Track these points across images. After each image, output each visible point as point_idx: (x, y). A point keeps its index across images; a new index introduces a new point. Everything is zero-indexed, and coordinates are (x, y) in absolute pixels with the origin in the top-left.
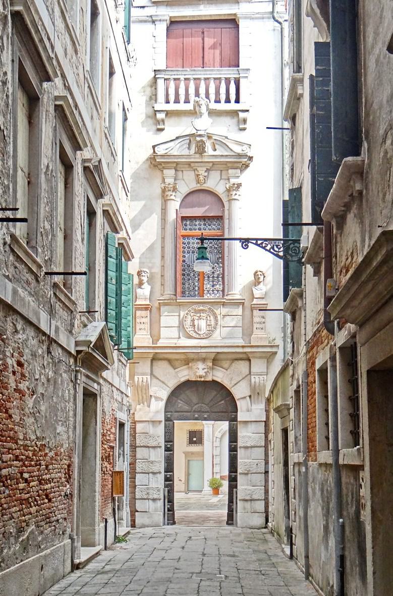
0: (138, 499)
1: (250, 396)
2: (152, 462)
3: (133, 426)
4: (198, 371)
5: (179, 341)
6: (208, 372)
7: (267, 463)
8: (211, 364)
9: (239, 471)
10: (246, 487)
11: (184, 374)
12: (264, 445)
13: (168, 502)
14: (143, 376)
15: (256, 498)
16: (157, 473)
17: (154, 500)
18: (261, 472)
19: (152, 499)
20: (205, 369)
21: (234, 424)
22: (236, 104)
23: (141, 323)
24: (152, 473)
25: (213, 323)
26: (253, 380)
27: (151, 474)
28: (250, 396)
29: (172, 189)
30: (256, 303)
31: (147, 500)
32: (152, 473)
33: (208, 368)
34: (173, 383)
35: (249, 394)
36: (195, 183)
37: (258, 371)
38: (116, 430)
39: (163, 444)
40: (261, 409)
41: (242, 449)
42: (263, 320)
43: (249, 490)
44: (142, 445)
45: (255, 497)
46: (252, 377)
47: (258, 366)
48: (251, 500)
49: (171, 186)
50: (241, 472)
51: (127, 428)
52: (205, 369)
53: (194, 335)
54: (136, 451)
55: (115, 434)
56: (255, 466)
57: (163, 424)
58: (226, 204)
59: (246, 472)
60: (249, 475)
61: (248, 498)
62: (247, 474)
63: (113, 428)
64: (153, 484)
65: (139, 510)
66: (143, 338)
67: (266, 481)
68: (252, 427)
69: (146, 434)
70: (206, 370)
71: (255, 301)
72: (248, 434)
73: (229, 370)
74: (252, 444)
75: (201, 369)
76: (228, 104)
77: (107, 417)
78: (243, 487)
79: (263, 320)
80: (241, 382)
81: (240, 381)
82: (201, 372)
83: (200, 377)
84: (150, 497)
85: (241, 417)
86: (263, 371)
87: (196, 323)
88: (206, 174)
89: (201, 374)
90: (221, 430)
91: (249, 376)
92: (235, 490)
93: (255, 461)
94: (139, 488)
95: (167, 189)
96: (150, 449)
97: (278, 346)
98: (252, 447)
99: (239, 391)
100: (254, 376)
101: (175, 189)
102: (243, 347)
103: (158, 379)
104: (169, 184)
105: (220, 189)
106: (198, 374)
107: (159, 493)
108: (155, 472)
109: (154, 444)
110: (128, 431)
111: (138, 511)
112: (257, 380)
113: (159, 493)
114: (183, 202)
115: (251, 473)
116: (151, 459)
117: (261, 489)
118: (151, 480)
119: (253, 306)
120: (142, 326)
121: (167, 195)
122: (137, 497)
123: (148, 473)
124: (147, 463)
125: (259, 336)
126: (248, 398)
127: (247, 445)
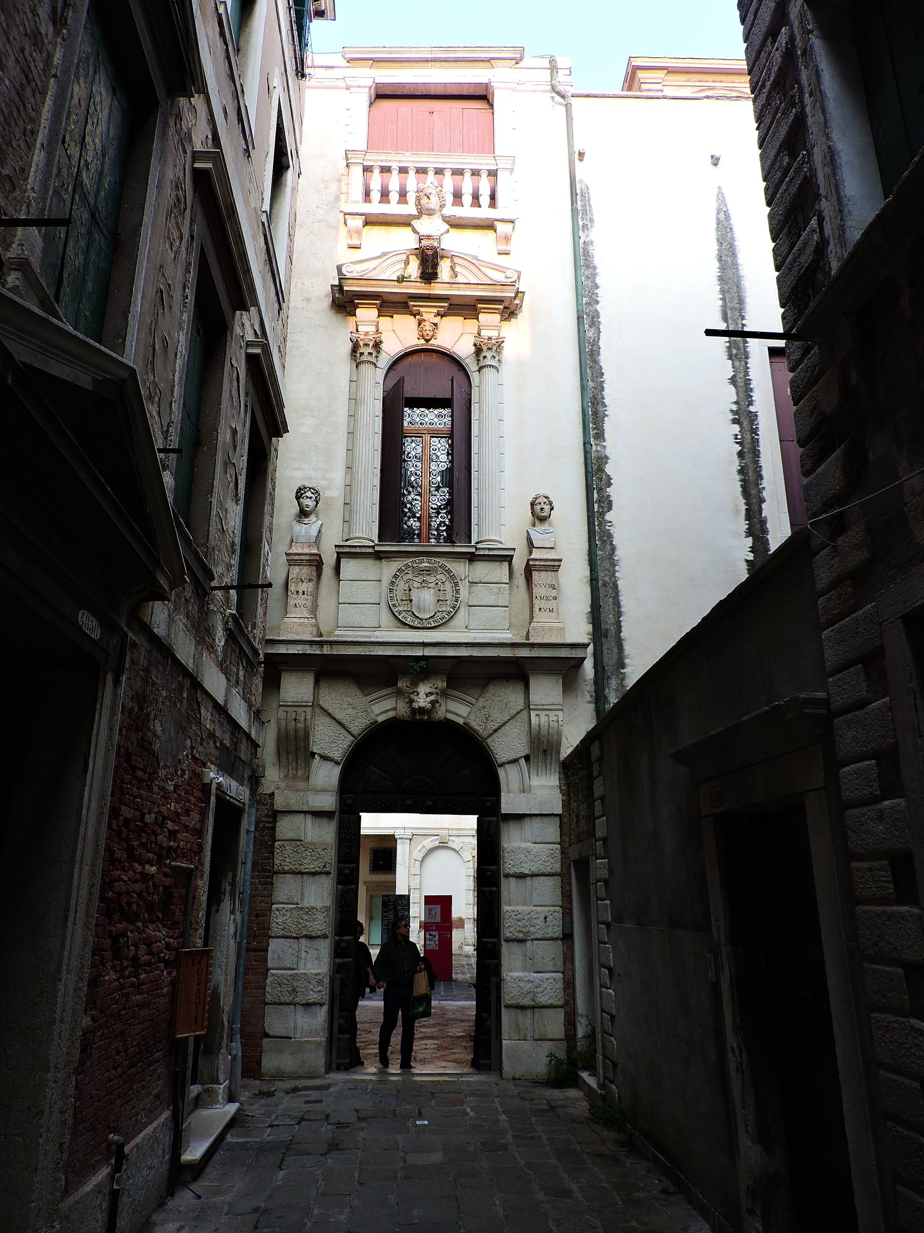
0: (270, 1004)
1: (527, 758)
2: (310, 911)
3: (268, 822)
4: (415, 698)
5: (376, 633)
6: (437, 702)
7: (567, 913)
8: (445, 684)
9: (507, 933)
10: (520, 974)
11: (383, 708)
12: (559, 870)
13: (341, 1010)
14: (299, 710)
15: (544, 1003)
16: (318, 937)
17: (307, 1005)
18: (555, 936)
19: (303, 1005)
20: (431, 694)
21: (490, 822)
22: (491, 209)
23: (298, 592)
24: (306, 936)
25: (449, 597)
26: (534, 720)
27: (303, 941)
28: (527, 758)
29: (371, 344)
30: (538, 557)
31: (293, 1007)
32: (306, 936)
33: (437, 694)
34: (358, 725)
35: (526, 752)
36: (417, 336)
37: (545, 702)
38: (203, 819)
39: (332, 868)
40: (550, 787)
41: (513, 881)
42: (554, 593)
43: (529, 981)
44: (286, 868)
45: (543, 999)
46: (533, 714)
47: (545, 691)
48: (533, 1007)
49: (371, 337)
50: (509, 935)
51: (248, 823)
52: (431, 694)
53: (409, 620)
54: (272, 884)
55: (199, 833)
56: (540, 922)
57: (337, 814)
58: (475, 378)
59: (521, 935)
60: (529, 944)
61: (526, 1001)
62: (522, 941)
63: (195, 816)
64: (309, 965)
65: (271, 1033)
66: (301, 624)
67: (569, 958)
68: (532, 828)
69: (298, 843)
70: (432, 698)
71: (536, 554)
72: (524, 845)
73: (481, 700)
74: (534, 869)
75: (422, 695)
76: (477, 209)
77: (162, 773)
78: (515, 974)
79: (554, 593)
80: (507, 727)
81: (504, 724)
82: (422, 701)
83: (420, 713)
84: (298, 1000)
85: (509, 803)
86: (555, 702)
87: (414, 595)
88: (437, 320)
89: (422, 704)
90: (422, 849)
91: (525, 713)
92: (493, 979)
93: (539, 909)
94: (273, 975)
95: (361, 343)
96: (305, 877)
97: (585, 646)
98: (533, 875)
99: (507, 745)
100: (538, 712)
101: (377, 345)
102: (514, 645)
103: (330, 715)
104: (367, 334)
105: (464, 349)
106: (415, 705)
107: (320, 988)
108: (313, 934)
109: (312, 867)
110: (248, 832)
111: (267, 1036)
112: (544, 719)
113: (320, 988)
114: (392, 372)
115: (532, 940)
116: (307, 903)
117: (555, 980)
118: (303, 955)
119: (531, 563)
120: (300, 600)
121: (362, 354)
122: (269, 998)
123: (297, 938)
124: (295, 913)
125: (546, 625)
126: (523, 761)
127: (522, 870)
